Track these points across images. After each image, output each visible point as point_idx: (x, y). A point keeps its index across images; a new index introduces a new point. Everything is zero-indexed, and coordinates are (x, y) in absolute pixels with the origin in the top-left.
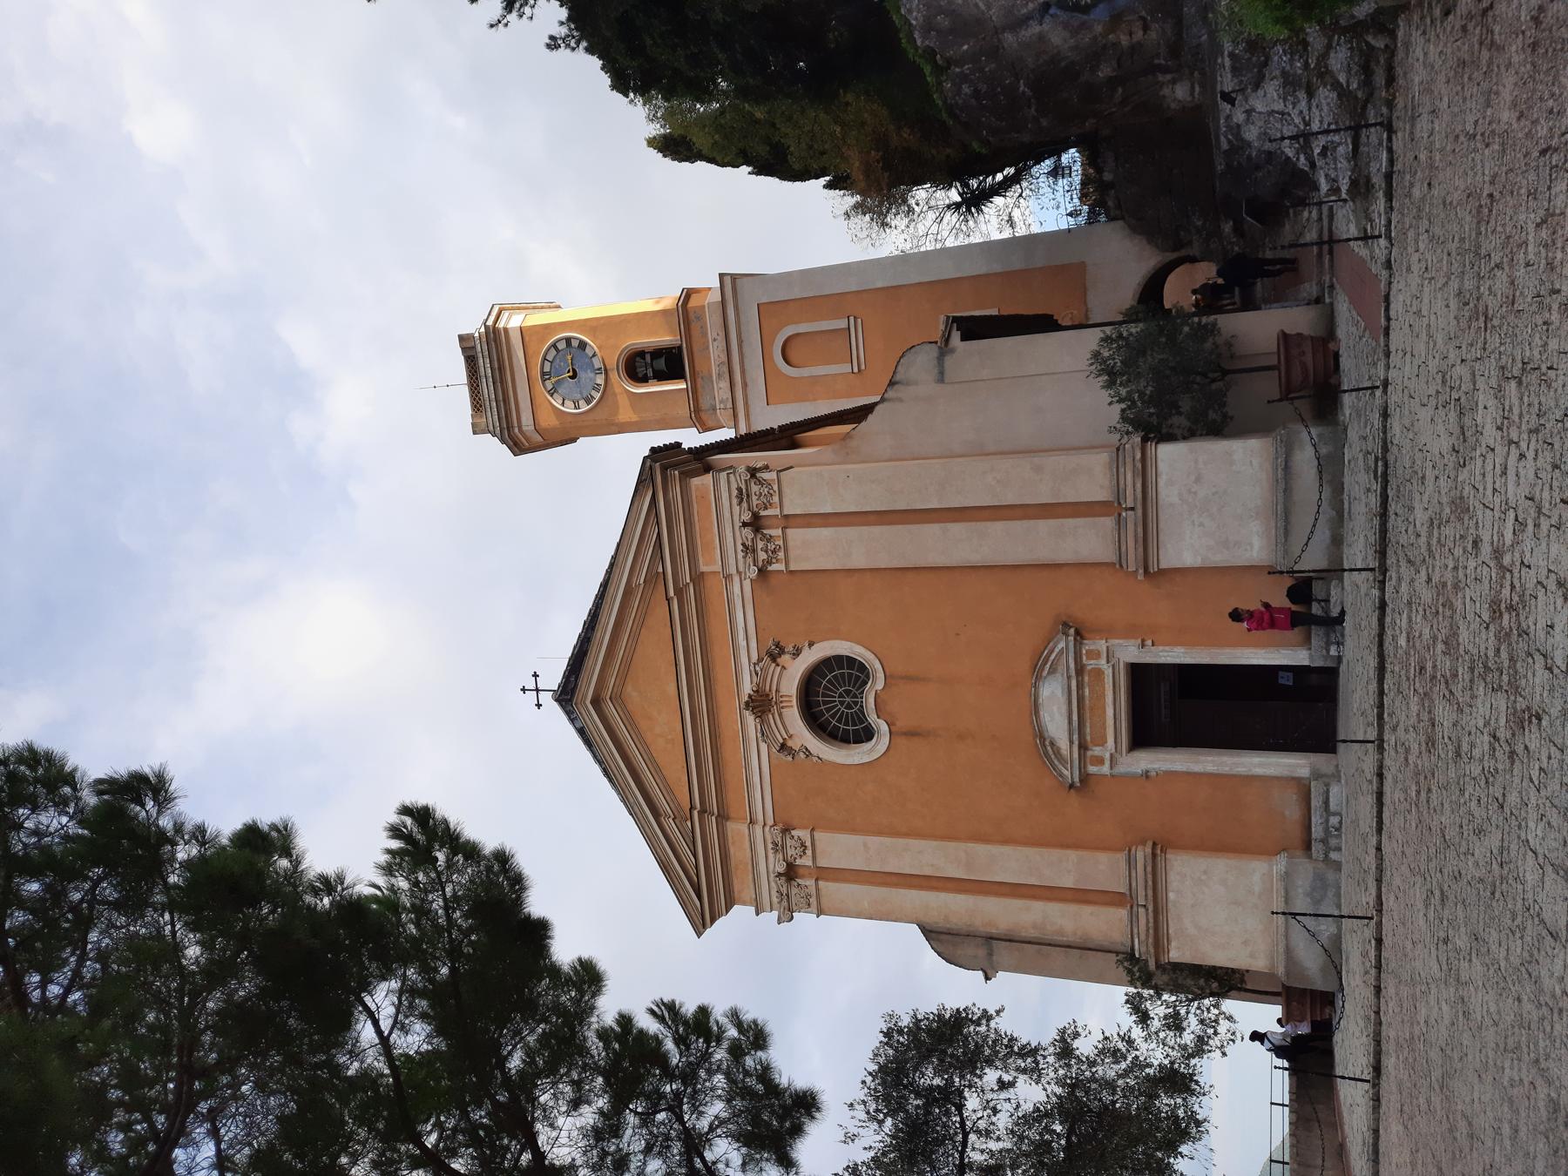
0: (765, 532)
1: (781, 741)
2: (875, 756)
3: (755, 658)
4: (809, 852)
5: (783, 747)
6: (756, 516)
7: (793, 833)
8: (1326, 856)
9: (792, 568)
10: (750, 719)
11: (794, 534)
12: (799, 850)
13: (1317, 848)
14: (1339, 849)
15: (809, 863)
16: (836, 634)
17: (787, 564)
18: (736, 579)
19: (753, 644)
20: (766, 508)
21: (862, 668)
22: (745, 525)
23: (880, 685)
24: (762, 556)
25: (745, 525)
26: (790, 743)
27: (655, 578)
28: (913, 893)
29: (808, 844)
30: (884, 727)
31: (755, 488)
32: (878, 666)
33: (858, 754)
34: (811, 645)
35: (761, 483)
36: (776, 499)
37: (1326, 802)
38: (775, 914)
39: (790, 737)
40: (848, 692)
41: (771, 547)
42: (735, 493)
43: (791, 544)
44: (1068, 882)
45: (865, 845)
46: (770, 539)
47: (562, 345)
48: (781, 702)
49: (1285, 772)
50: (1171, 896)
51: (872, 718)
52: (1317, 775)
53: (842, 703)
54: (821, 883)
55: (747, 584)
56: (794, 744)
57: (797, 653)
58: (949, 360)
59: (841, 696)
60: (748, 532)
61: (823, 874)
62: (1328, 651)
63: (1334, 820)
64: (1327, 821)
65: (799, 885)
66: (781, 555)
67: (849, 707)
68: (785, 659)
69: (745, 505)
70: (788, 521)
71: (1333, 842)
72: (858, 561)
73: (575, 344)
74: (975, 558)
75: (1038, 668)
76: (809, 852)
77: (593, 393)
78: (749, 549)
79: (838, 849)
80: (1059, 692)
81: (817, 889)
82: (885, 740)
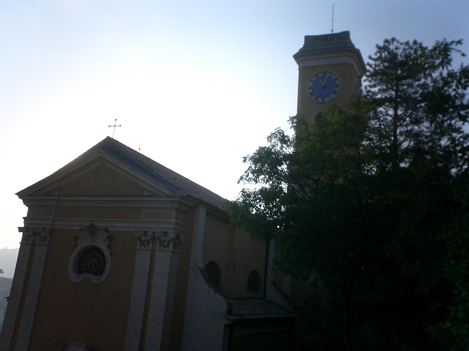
0: (152, 241)
1: (80, 236)
3: (110, 229)
6: (158, 239)
7: (49, 237)
24: (143, 239)
29: (44, 242)
34: (111, 254)
35: (169, 243)
36: (162, 248)
41: (146, 243)
46: (149, 243)
47: (337, 82)
48: (93, 238)
57: (109, 247)
66: (143, 247)
68: (108, 242)
69: (162, 234)
70: (153, 252)
73: (337, 89)
77: (314, 96)
78: (146, 233)
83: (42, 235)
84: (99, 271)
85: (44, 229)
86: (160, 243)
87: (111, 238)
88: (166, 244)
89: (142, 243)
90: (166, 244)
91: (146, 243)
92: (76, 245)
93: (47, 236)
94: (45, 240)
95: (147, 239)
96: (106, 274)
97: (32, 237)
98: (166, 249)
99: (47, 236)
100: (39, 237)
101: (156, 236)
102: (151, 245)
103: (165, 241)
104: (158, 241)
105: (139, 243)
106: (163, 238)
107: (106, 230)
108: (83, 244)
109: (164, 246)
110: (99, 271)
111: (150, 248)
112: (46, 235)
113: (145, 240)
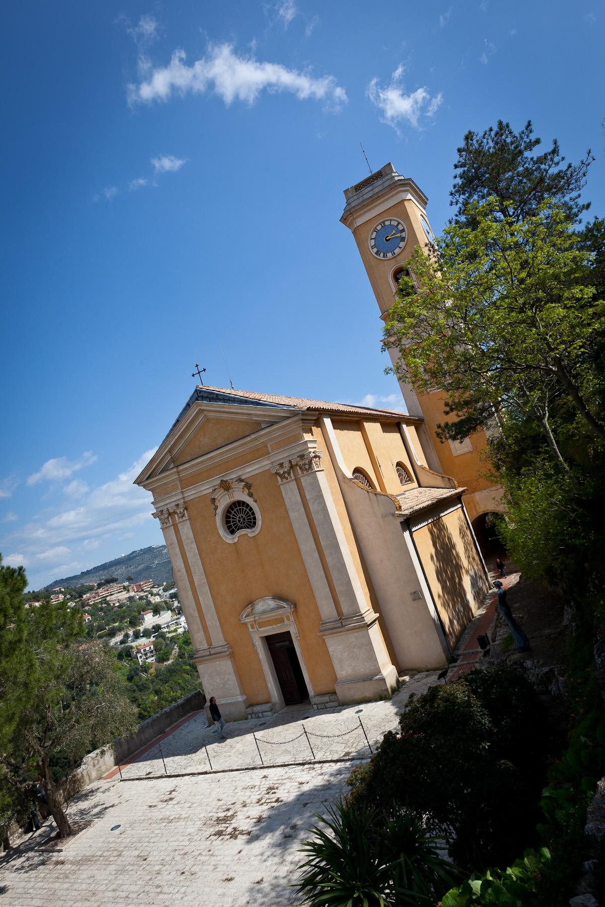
2: (224, 539)
3: (243, 477)
4: (181, 520)
5: (214, 499)
6: (297, 465)
7: (185, 511)
8: (249, 714)
9: (282, 487)
10: (219, 482)
11: (293, 485)
12: (180, 515)
13: (249, 710)
14: (252, 718)
15: (178, 521)
16: (263, 511)
17: (282, 484)
18: (269, 462)
19: (248, 476)
20: (300, 469)
21: (255, 523)
22: (290, 462)
23: (250, 535)
25: (290, 462)
26: (217, 501)
27: (258, 423)
28: (183, 566)
29: (184, 519)
30: (236, 540)
31: (307, 462)
32: (257, 533)
33: (222, 531)
34: (255, 501)
37: (265, 712)
38: (155, 511)
39: (219, 501)
40: (244, 519)
41: (286, 475)
42: (302, 454)
43: (290, 484)
44: (208, 624)
45: (192, 542)
46: (289, 474)
49: (272, 693)
50: (218, 663)
51: (239, 533)
52: (274, 704)
53: (239, 518)
54: (172, 527)
55: (267, 468)
56: (217, 503)
57: (250, 495)
58: (391, 517)
59: (242, 517)
60: (287, 465)
61: (175, 526)
62: (315, 704)
63: (260, 715)
64: (259, 713)
65: (168, 518)
66: (285, 481)
67: (239, 521)
68: (246, 491)
69: (298, 459)
70: (297, 480)
71: (253, 715)
72: (293, 515)
74: (308, 566)
75: (278, 597)
76: (181, 520)
78: (281, 465)
79: (186, 529)
80: (271, 607)
81: (170, 526)
82: (230, 542)
83: (178, 512)
84: (251, 523)
85: (177, 505)
86: (301, 468)
87: (248, 486)
88: (307, 467)
89: (282, 476)
90: (307, 467)
91: (286, 475)
92: (216, 508)
93: (184, 511)
94: (183, 516)
95: (286, 470)
96: (259, 523)
97: (170, 518)
98: (310, 471)
99: (184, 511)
100: (176, 515)
101: (294, 463)
102: (292, 475)
103: (305, 464)
104: (298, 468)
105: (279, 478)
106: (301, 463)
107: (240, 480)
108: (224, 502)
109: (306, 470)
110: (251, 523)
111: (293, 478)
112: (182, 511)
113: (284, 473)
